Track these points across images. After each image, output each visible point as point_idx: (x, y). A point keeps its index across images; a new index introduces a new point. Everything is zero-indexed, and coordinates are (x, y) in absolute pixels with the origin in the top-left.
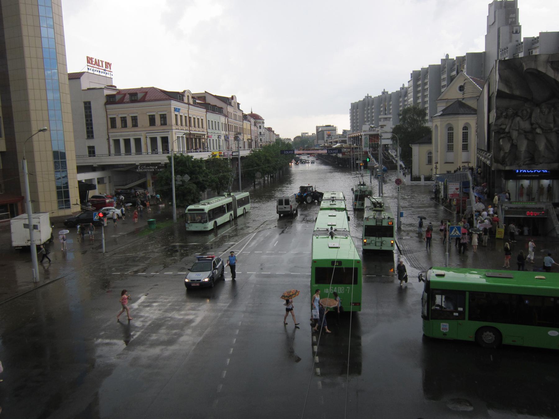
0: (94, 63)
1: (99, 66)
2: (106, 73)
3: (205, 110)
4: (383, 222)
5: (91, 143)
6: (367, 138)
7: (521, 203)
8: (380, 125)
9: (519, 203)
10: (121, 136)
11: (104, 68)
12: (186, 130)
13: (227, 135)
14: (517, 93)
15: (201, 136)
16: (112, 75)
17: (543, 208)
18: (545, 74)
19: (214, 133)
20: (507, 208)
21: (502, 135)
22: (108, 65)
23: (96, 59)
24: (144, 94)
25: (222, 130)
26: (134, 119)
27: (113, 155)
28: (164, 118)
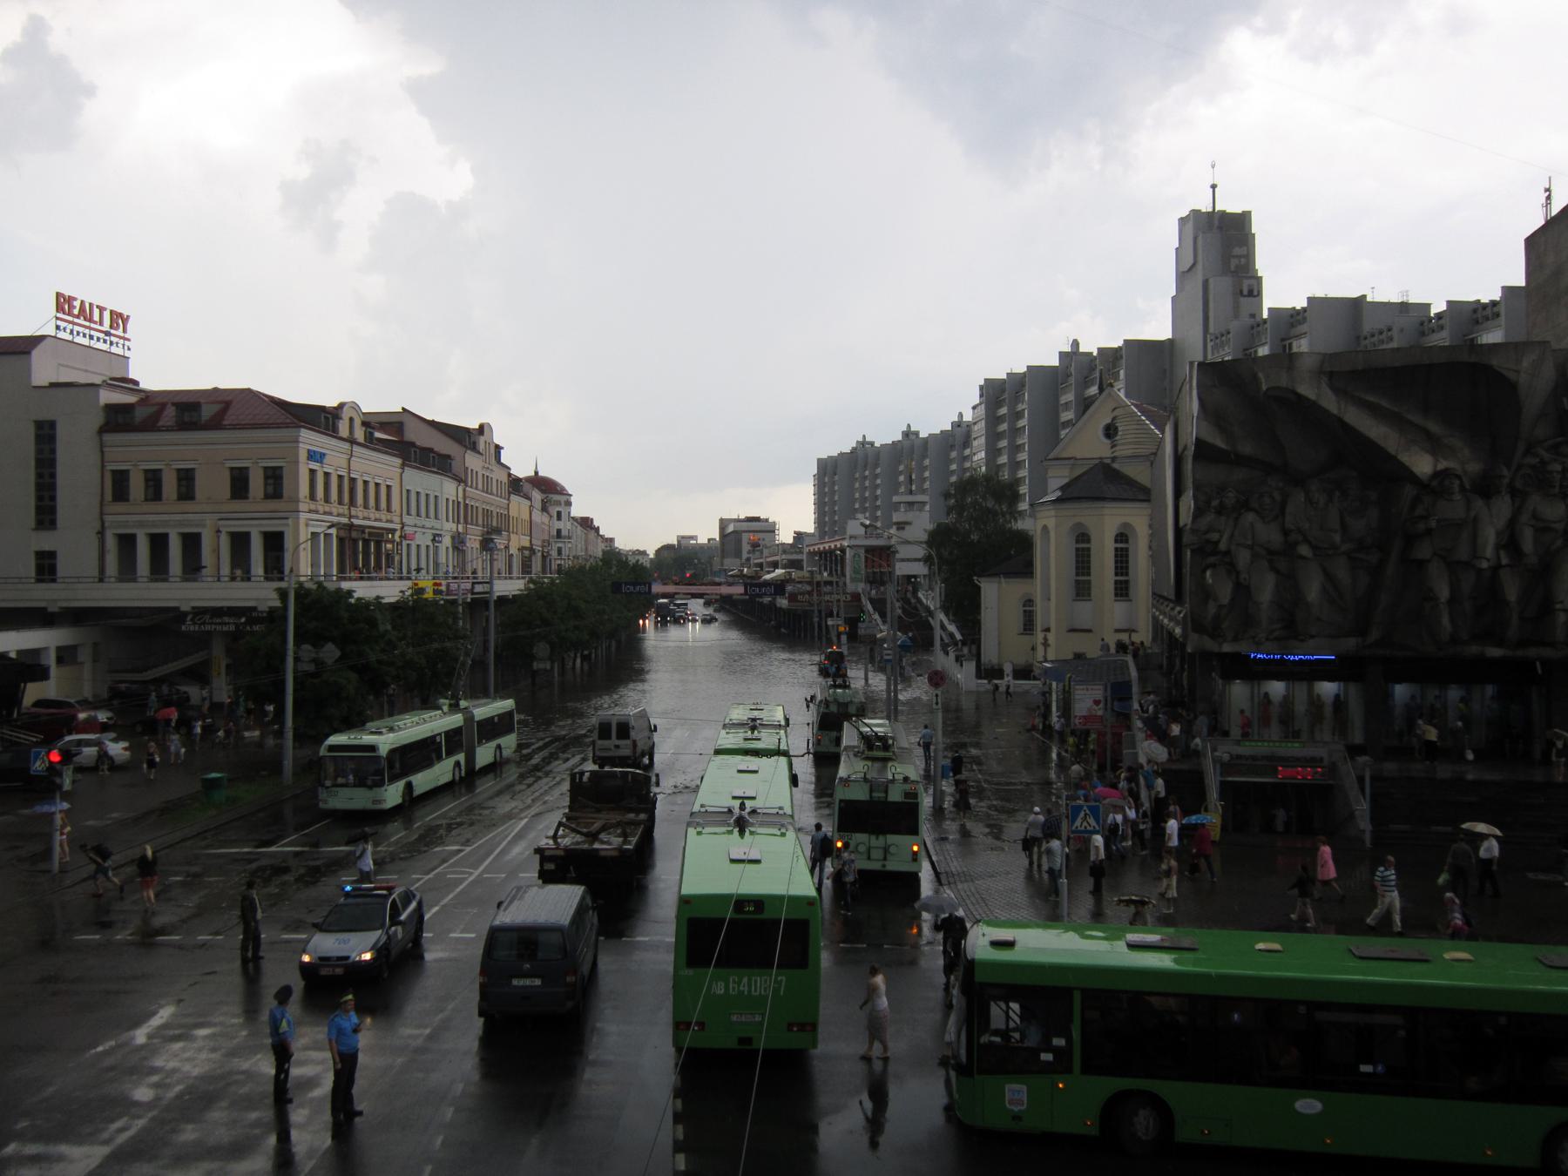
0: (76, 312)
1: (91, 320)
2: (111, 343)
3: (398, 461)
4: (890, 792)
5: (46, 542)
6: (859, 556)
7: (1266, 744)
8: (894, 520)
9: (1260, 744)
10: (141, 524)
11: (106, 327)
12: (338, 515)
13: (459, 533)
14: (1246, 448)
15: (383, 534)
16: (129, 349)
17: (1321, 759)
19: (423, 527)
20: (1226, 757)
21: (1212, 560)
22: (119, 319)
23: (82, 302)
24: (222, 406)
25: (447, 520)
26: (186, 479)
27: (113, 580)
28: (275, 481)
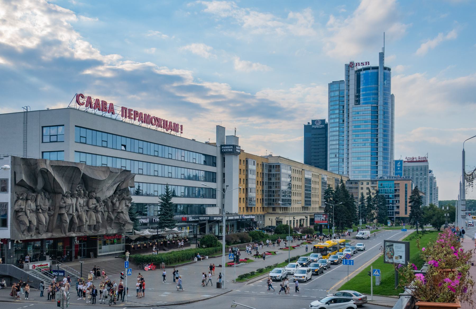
18: (51, 173)
